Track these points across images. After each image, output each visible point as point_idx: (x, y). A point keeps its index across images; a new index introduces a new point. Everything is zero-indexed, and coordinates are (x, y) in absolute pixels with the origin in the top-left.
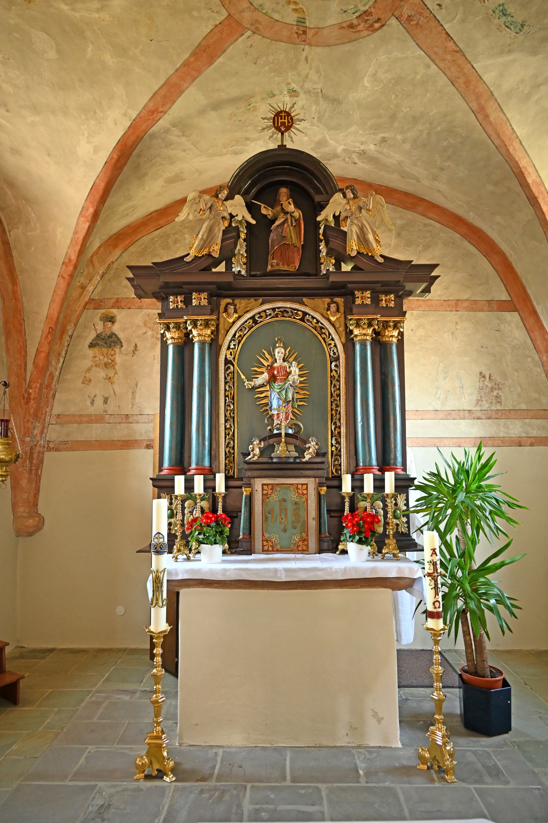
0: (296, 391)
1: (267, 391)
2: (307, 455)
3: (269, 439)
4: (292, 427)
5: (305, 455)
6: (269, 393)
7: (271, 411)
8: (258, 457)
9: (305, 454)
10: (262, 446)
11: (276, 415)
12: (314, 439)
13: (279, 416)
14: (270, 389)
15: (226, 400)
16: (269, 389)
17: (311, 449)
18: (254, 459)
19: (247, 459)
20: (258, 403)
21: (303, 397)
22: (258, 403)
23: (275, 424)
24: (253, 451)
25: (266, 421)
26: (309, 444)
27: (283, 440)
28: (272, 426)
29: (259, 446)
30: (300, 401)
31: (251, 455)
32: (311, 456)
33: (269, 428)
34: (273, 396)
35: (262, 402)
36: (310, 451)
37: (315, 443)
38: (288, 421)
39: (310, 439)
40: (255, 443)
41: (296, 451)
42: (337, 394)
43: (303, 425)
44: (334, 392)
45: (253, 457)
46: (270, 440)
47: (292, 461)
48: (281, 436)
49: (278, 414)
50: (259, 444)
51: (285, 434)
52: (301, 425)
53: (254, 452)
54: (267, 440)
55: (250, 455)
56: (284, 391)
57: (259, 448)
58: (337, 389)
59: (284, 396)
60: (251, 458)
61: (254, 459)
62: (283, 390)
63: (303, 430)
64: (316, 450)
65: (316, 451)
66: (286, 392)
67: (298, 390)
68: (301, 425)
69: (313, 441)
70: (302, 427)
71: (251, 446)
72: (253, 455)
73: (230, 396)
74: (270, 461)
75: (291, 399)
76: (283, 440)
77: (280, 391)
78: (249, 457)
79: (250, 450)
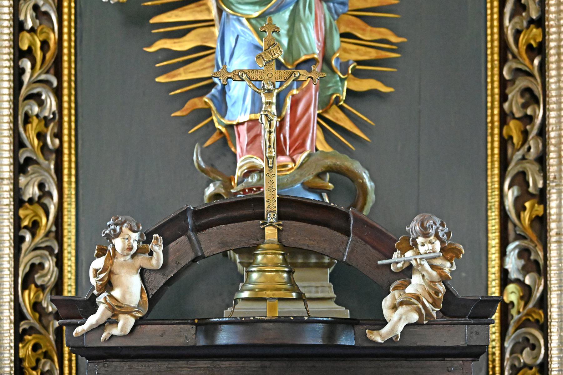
0: (344, 29)
1: (209, 23)
2: (394, 308)
3: (198, 229)
4: (319, 183)
5: (386, 312)
6: (216, 31)
7: (223, 110)
8: (139, 322)
9: (386, 303)
10: (157, 260)
11: (243, 129)
12: (434, 223)
13: (258, 136)
14: (220, 11)
15: (18, 73)
16: (214, 14)
17: (416, 279)
18: (116, 331)
19: (79, 330)
20: (161, 79)
21: (372, 54)
22: (161, 79)
23: (238, 173)
24: (108, 286)
25: (197, 158)
26: (409, 254)
27: (271, 233)
28: (227, 183)
29: (142, 260)
30: (357, 74)
31: (102, 308)
32: (415, 317)
33: (210, 190)
34: (230, 41)
35: (183, 75)
36: (409, 290)
37: (438, 245)
38: (300, 158)
39: (415, 226)
40: (118, 243)
41: (337, 302)
42: (529, 47)
43: (372, 178)
44: (517, 33)
45: (112, 321)
46: (201, 235)
47: (319, 342)
48: (261, 217)
49: (253, 124)
50: (140, 251)
51: (282, 201)
52: (366, 176)
53: (116, 293)
54: (184, 232)
55: (94, 312)
56: (286, 15)
57: (143, 272)
58: (531, 22)
59: (285, 41)
60: (101, 327)
61: (116, 331)
62: (279, 8)
63: (372, 197)
64: (444, 280)
65: (442, 288)
66: (294, 19)
67: (348, 23)
68: (366, 176)
69: (426, 235)
70: (369, 184)
71: (99, 263)
72: (111, 308)
73: (39, 54)
74: (202, 342)
75: (317, 53)
76: (271, 233)
77: (262, 16)
78: (92, 320)
79: (93, 281)
